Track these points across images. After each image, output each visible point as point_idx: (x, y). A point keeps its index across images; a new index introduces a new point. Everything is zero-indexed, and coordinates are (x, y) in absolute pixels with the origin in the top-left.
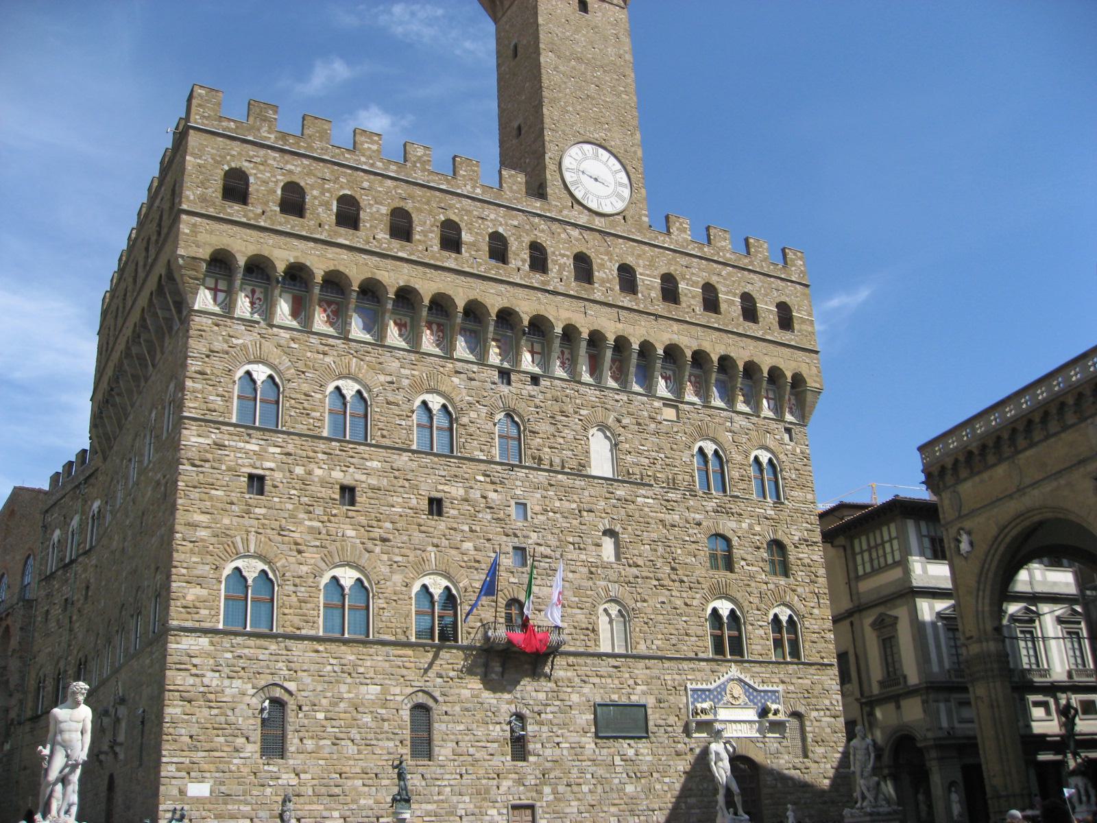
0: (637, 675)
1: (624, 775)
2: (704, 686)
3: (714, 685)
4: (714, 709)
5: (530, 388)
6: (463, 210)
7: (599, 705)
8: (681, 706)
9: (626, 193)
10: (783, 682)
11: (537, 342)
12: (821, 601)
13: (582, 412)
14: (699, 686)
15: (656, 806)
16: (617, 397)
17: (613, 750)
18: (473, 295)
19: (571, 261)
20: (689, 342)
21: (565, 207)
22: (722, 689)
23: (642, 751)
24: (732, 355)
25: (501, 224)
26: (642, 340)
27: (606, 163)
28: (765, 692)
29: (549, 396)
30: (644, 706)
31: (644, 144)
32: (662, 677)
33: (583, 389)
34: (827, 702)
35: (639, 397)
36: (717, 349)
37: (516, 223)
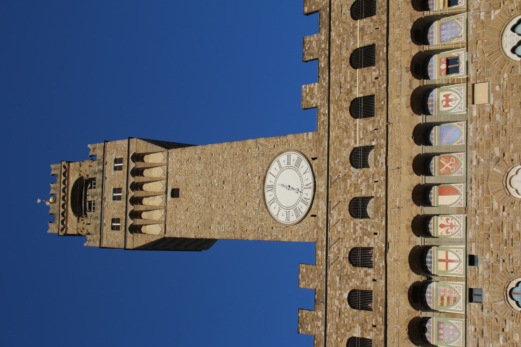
5: (481, 266)
6: (337, 333)
9: (294, 156)
11: (437, 256)
13: (496, 205)
16: (475, 163)
18: (404, 333)
19: (358, 221)
20: (404, 84)
21: (316, 223)
24: (410, 27)
25: (341, 294)
26: (412, 140)
27: (276, 177)
29: (485, 246)
31: (255, 136)
33: (473, 205)
35: (471, 134)
36: (408, 47)
37: (338, 278)
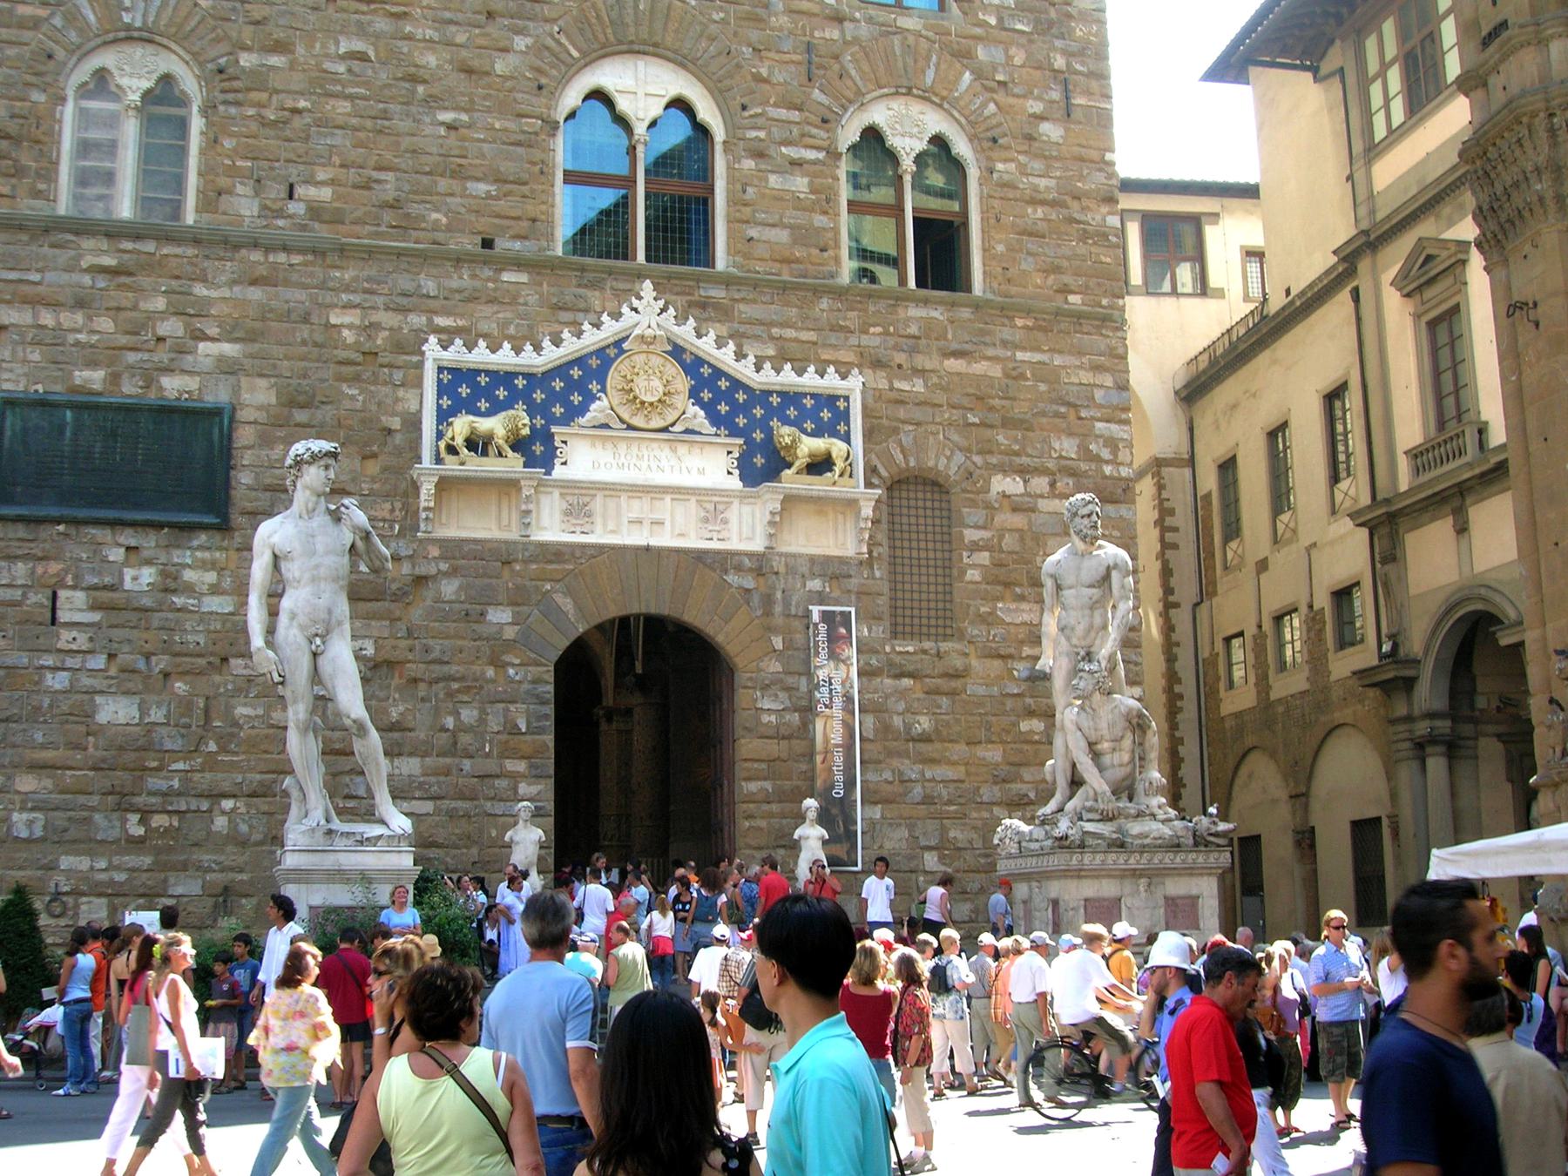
0: (209, 302)
1: (99, 662)
2: (505, 358)
3: (551, 355)
4: (537, 449)
7: (11, 402)
8: (395, 423)
10: (877, 364)
12: (1079, 100)
14: (481, 356)
15: (225, 781)
17: (54, 567)
22: (589, 373)
23: (189, 575)
28: (791, 398)
30: (215, 413)
32: (315, 319)
34: (1067, 446)
